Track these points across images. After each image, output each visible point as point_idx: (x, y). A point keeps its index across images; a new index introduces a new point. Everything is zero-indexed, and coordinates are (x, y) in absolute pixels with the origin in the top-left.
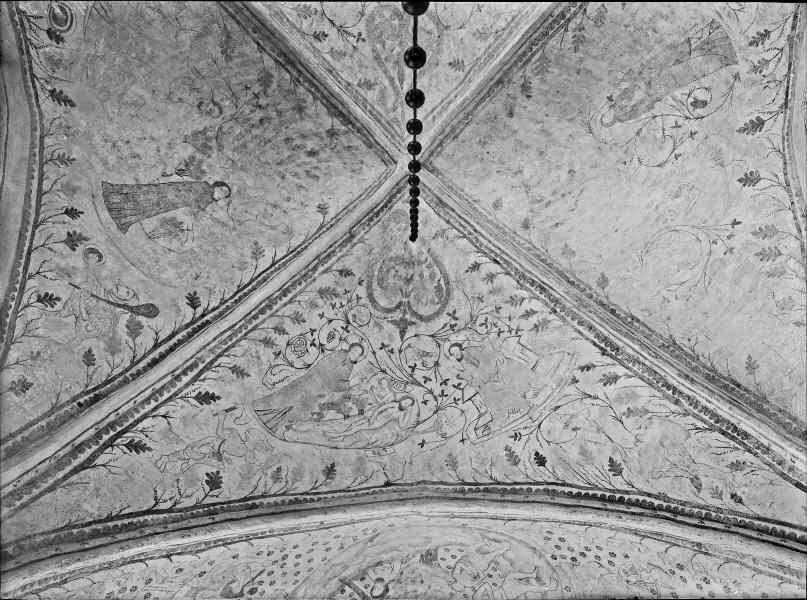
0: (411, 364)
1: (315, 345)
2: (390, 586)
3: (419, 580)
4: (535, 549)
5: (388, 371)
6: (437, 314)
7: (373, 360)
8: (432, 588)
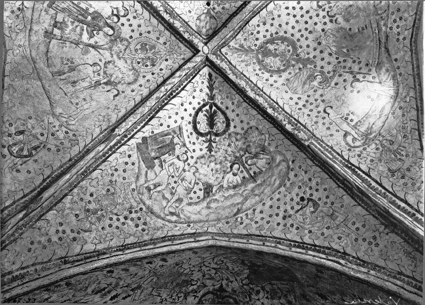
0: (217, 275)
1: (266, 291)
2: (229, 170)
3: (214, 172)
4: (152, 213)
5: (229, 273)
6: (204, 295)
7: (237, 277)
8: (207, 165)
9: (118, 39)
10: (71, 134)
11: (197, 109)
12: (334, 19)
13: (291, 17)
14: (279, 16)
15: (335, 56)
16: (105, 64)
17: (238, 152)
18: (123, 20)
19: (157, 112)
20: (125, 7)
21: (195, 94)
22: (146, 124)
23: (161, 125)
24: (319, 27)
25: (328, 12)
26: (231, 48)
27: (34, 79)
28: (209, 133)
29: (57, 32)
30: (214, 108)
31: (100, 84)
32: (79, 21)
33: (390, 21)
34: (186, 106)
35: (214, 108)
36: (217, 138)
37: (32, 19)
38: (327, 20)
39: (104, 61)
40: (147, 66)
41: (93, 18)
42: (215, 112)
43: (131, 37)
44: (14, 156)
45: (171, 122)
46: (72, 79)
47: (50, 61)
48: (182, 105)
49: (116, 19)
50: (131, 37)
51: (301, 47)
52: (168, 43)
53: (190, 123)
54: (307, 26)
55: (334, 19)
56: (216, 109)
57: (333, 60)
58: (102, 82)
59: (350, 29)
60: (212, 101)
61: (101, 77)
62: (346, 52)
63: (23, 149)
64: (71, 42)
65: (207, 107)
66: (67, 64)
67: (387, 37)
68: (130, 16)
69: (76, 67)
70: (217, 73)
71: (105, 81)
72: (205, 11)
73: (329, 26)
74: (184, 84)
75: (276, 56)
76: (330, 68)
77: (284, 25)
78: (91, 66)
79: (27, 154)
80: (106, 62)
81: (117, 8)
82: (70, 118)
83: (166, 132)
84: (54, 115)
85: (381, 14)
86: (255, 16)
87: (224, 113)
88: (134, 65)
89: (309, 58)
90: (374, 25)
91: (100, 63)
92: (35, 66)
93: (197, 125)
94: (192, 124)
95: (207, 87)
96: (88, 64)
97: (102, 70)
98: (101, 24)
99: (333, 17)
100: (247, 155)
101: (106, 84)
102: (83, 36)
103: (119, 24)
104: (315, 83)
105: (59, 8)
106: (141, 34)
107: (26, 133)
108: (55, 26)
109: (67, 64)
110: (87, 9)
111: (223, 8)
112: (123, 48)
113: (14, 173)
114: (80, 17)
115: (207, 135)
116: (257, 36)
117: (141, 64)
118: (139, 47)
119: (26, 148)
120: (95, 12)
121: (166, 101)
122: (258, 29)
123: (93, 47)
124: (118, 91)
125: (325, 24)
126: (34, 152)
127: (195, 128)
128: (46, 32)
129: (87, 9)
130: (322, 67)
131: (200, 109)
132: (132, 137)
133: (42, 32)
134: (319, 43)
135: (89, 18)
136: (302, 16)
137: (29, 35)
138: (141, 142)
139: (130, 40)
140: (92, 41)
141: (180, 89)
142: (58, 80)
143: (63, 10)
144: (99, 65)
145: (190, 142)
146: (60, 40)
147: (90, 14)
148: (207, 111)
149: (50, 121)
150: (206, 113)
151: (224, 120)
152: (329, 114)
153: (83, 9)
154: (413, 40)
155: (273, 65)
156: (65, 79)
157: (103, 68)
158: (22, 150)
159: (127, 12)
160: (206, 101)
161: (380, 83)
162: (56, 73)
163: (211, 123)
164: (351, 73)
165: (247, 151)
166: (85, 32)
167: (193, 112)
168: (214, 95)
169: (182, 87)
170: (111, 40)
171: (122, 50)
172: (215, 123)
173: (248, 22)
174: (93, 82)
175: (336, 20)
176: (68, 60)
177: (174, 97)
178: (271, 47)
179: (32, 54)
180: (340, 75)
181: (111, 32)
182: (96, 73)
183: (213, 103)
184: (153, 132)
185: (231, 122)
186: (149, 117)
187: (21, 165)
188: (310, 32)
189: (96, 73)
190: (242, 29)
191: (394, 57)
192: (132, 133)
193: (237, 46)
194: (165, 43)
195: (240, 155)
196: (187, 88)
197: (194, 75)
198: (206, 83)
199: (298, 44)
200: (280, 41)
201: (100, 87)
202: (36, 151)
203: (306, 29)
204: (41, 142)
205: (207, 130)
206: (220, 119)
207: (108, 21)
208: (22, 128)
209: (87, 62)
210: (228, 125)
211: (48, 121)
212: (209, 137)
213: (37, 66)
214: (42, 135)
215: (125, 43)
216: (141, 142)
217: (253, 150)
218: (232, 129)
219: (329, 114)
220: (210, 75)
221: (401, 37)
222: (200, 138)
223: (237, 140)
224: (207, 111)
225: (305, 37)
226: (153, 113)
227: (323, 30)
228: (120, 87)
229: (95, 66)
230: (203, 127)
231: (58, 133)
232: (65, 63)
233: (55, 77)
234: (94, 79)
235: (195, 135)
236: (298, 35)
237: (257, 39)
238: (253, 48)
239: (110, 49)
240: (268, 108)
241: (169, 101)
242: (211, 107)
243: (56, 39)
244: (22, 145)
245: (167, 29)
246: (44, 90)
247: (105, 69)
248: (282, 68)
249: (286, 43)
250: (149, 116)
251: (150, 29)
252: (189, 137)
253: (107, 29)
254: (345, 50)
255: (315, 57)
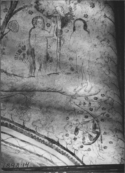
16: (38, 10)
27: (32, 96)
31: (61, 31)
39: (33, 9)
44: (93, 143)
47: (17, 74)
58: (60, 28)
61: (53, 24)
63: (90, 135)
66: (24, 55)
69: (30, 46)
71: (59, 23)
78: (34, 27)
79: (96, 135)
80: (35, 7)
82: (83, 85)
91: (34, 15)
92: (19, 91)
96: (31, 30)
97: (44, 18)
107: (78, 127)
113: (105, 150)
119: (91, 133)
124: (80, 19)
142: (40, 74)
144: (37, 18)
149: (78, 104)
157: (41, 15)
158: (90, 136)
174: (56, 37)
179: (6, 90)
182: (46, 27)
187: (102, 143)
189: (46, 27)
201: (64, 33)
202: (97, 128)
204: (92, 121)
208: (74, 128)
209: (29, 30)
211: (76, 105)
213: (20, 89)
229: (36, 24)
232: (22, 57)
233: (35, 75)
234: (52, 33)
244: (87, 134)
246: (45, 91)
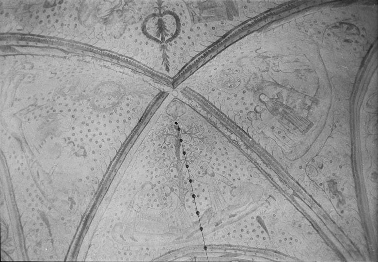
9: (256, 90)
10: (303, 30)
11: (178, 37)
12: (68, 141)
13: (103, 133)
14: (114, 131)
15: (57, 111)
17: (130, 7)
18: (252, 109)
19: (218, 41)
20: (250, 120)
21: (181, 52)
22: (230, 32)
23: (213, 28)
24: (77, 130)
25: (74, 145)
26: (150, 95)
28: (162, 15)
29: (309, 103)
30: (160, 39)
31: (273, 57)
32: (290, 108)
33: (25, 163)
34: (189, 42)
35: (160, 39)
36: (153, 12)
37: (327, 116)
38: (73, 139)
39: (269, 73)
40: (229, 69)
41: (277, 109)
42: (158, 35)
43: (244, 92)
45: (203, 29)
46: (298, 64)
48: (193, 43)
49: (258, 108)
50: (244, 92)
51: (88, 108)
52: (210, 90)
53: (184, 25)
54: (88, 128)
55: (68, 141)
56: (158, 38)
57: (58, 108)
59: (52, 138)
60: (163, 44)
62: (49, 119)
64: (297, 91)
65: (166, 38)
66: (302, 76)
67: (22, 149)
68: (245, 112)
70: (162, 73)
72: (178, 118)
73: (69, 134)
74: (193, 62)
75: (107, 94)
76: (58, 101)
77: (108, 123)
81: (257, 119)
83: (208, 20)
84: (317, 44)
85: (33, 163)
86: (135, 128)
87: (150, 37)
88: (241, 69)
89: (78, 101)
90: (35, 152)
93: (175, 22)
94: (182, 24)
95: (169, 58)
98: (270, 104)
99: (69, 143)
100: (121, 8)
101: (267, 57)
102: (287, 95)
103: (255, 105)
104: (68, 86)
105: (305, 121)
106: (236, 96)
108: (309, 107)
109: (302, 76)
110: (282, 118)
111: (162, 125)
112: (251, 82)
114: (288, 112)
115: (163, 13)
116: (128, 109)
117: (235, 70)
118: (237, 84)
120: (275, 115)
121: (210, 49)
122: (129, 115)
123: (278, 84)
125: (73, 135)
126: (338, 24)
127: (177, 19)
128: (317, 104)
129: (282, 118)
130: (65, 99)
131: (174, 36)
132: (244, 23)
133: (321, 104)
134: (73, 116)
135: (281, 110)
136: (94, 135)
137: (331, 105)
138: (234, 17)
139: (245, 89)
140: (279, 89)
141: (197, 59)
143: (301, 119)
144: (274, 70)
145: (182, 6)
146: (306, 95)
147: (280, 113)
148: (167, 35)
150: (168, 33)
151: (148, 31)
152: (52, 73)
153: (285, 118)
154: (5, 161)
155: (110, 87)
156: (304, 65)
159: (248, 116)
160: (168, 44)
161: (14, 114)
162: (312, 72)
163: (161, 27)
164: (39, 107)
165: (122, 11)
166: (285, 99)
167: (181, 34)
168: (161, 50)
169: (195, 60)
170: (262, 89)
171: (252, 79)
172: (157, 25)
173: (140, 121)
175: (65, 140)
176: (301, 78)
177: (202, 52)
178: (114, 100)
180: (48, 100)
181: (262, 97)
183: (161, 43)
184: (222, 23)
185: (142, 32)
186: (227, 38)
188: (83, 123)
190: (143, 114)
191: (12, 138)
192: (243, 26)
193: (145, 96)
194: (213, 90)
195: (128, 5)
196: (189, 59)
197: (184, 70)
198: (170, 61)
199: (91, 110)
200: (107, 107)
203: (87, 125)
205: (164, 17)
206: (152, 29)
207: (264, 107)
208: (345, 44)
210: (144, 28)
212: (162, 11)
214: (329, 35)
215: (249, 87)
216: (234, 17)
217: (115, 14)
218: (139, 25)
219: (52, 73)
220: (167, 69)
221: (13, 156)
222: (171, 10)
223: (133, 17)
224: (167, 35)
225: (87, 118)
226: (222, 41)
227: (73, 128)
228: (254, 54)
230: (169, 21)
231: (314, 32)
235: (177, 13)
236: (93, 117)
237: (128, 105)
238: (130, 97)
239: (263, 81)
240: (110, 65)
241: (207, 49)
242: (163, 38)
243: (309, 96)
245: (212, 104)
246: (323, 63)
247: (268, 66)
248: (100, 87)
249: (102, 107)
250: (226, 40)
251: (227, 102)
252: (184, 11)
253: (265, 99)
254: (50, 120)
255: (74, 104)
